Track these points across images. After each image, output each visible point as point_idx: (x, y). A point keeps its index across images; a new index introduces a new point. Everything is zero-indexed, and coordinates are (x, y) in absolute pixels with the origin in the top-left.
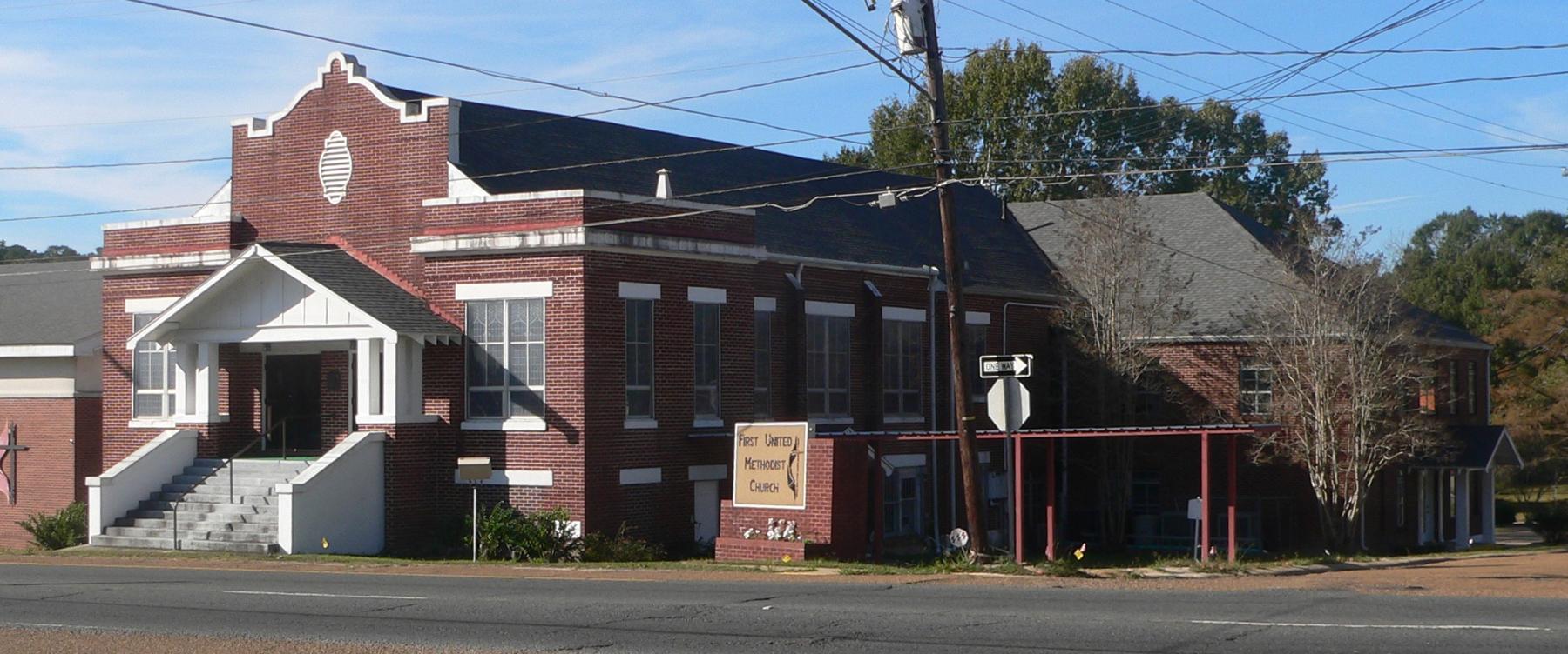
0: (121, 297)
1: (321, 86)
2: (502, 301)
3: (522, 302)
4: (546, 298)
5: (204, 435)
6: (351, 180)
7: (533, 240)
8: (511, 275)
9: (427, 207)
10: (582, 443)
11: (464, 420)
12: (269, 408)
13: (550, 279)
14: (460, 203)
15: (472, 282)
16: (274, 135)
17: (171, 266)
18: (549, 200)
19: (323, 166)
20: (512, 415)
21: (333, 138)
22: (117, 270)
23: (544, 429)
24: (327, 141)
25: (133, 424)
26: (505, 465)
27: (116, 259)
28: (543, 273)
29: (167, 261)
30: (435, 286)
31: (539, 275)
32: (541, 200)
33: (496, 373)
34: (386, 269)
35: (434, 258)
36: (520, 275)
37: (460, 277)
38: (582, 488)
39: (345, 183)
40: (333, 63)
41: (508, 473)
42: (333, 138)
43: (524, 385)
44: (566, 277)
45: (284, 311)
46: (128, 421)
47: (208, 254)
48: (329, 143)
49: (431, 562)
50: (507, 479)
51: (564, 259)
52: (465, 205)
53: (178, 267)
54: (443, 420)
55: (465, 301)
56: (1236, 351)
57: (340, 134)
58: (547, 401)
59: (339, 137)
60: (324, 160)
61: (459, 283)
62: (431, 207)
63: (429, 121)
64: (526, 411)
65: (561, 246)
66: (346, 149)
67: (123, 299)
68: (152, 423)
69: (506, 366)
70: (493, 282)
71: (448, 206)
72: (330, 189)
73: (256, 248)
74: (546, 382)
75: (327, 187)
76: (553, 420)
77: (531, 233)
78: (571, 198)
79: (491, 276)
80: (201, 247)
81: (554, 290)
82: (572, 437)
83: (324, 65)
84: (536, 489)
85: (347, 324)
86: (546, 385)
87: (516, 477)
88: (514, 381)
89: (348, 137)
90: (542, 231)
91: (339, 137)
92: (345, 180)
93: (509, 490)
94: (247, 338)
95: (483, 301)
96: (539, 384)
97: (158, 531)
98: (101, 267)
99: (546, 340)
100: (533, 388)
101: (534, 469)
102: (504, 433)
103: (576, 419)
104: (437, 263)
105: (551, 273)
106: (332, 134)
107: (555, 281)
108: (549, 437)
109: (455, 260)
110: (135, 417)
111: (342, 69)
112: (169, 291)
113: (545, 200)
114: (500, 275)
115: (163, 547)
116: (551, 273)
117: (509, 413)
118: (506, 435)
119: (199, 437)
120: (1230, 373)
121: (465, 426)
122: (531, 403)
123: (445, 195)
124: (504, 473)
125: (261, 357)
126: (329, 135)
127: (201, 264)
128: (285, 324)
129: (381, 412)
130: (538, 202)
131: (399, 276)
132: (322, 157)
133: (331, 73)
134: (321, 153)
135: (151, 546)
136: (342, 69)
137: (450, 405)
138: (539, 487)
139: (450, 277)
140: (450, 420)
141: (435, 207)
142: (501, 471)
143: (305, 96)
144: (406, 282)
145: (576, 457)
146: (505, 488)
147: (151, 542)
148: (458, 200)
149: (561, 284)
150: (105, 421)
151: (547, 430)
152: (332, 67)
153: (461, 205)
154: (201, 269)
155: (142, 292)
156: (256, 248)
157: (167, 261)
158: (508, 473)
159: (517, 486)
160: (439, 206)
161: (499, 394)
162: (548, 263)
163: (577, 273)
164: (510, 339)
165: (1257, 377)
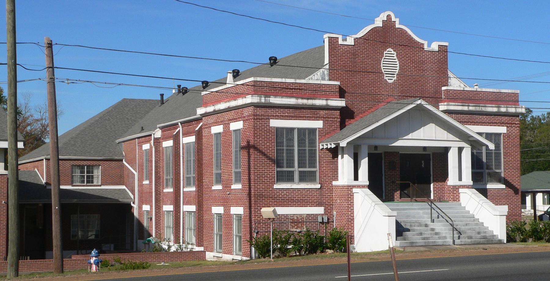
7: (503, 110)
8: (489, 123)
13: (506, 126)
15: (471, 125)
18: (504, 93)
21: (388, 51)
24: (385, 52)
25: (275, 186)
27: (270, 97)
31: (501, 124)
32: (501, 93)
35: (452, 113)
36: (493, 123)
40: (387, 16)
43: (492, 169)
46: (273, 185)
48: (386, 54)
52: (466, 91)
57: (392, 50)
67: (269, 119)
68: (291, 186)
71: (458, 90)
78: (514, 93)
89: (396, 52)
94: (391, 144)
97: (429, 237)
98: (259, 100)
104: (453, 115)
106: (388, 50)
107: (507, 127)
111: (393, 20)
112: (301, 117)
113: (503, 93)
115: (444, 244)
118: (487, 190)
126: (386, 50)
127: (327, 105)
136: (393, 20)
147: (438, 242)
152: (387, 18)
153: (464, 91)
155: (283, 116)
163: (517, 124)
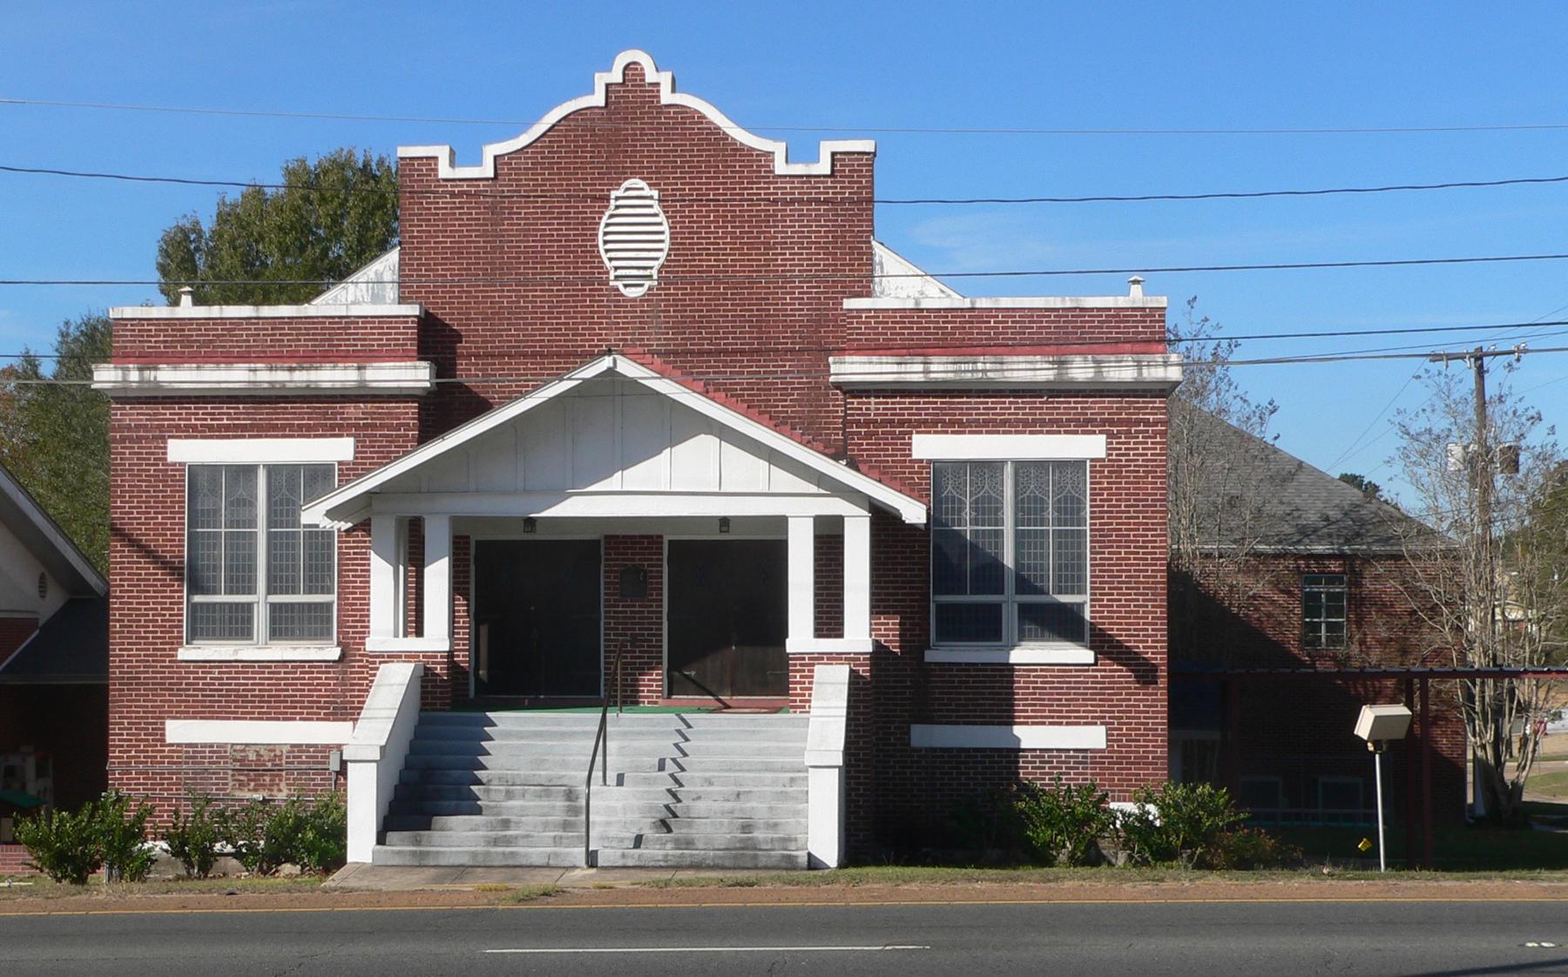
0: (162, 435)
1: (602, 104)
2: (1003, 462)
3: (1041, 465)
4: (340, 463)
5: (438, 671)
6: (667, 260)
7: (1081, 371)
8: (1026, 423)
9: (851, 310)
10: (1163, 682)
11: (929, 648)
12: (484, 629)
13: (1101, 432)
14: (922, 306)
15: (946, 432)
16: (496, 178)
17: (289, 385)
18: (1099, 309)
19: (606, 234)
20: (1021, 640)
21: (627, 189)
22: (1072, 382)
23: (1092, 661)
24: (614, 194)
25: (184, 653)
26: (1014, 717)
27: (156, 369)
28: (1088, 422)
29: (281, 376)
30: (868, 435)
31: (1083, 425)
32: (1082, 309)
33: (990, 575)
34: (745, 405)
35: (869, 391)
36: (1043, 423)
37: (920, 423)
38: (1162, 752)
39: (656, 264)
40: (626, 67)
41: (1018, 730)
42: (627, 189)
43: (1042, 591)
44: (1133, 429)
45: (623, 469)
46: (176, 650)
47: (374, 368)
48: (617, 198)
49: (1545, 874)
50: (1019, 740)
51: (1126, 402)
52: (928, 310)
53: (308, 387)
54: (887, 647)
55: (929, 461)
56: (1298, 567)
57: (643, 184)
58: (1092, 618)
59: (642, 189)
60: (608, 225)
61: (918, 432)
62: (858, 310)
63: (832, 175)
64: (1047, 634)
65: (1136, 382)
66: (657, 209)
67: (164, 439)
68: (236, 652)
69: (1009, 560)
70: (1005, 432)
71: (895, 310)
72: (620, 272)
73: (615, 361)
74: (1092, 588)
75: (616, 268)
76: (1104, 645)
77: (1078, 358)
78: (1143, 309)
79: (986, 423)
80: (364, 357)
81: (1108, 449)
82: (1144, 673)
83: (608, 68)
84: (1072, 753)
85: (766, 491)
86: (1092, 594)
87: (1030, 736)
88: (1024, 585)
89: (660, 190)
90: (1099, 357)
91: (642, 189)
92: (657, 259)
93: (1018, 757)
94: (538, 513)
95: (965, 462)
96: (1079, 593)
97: (516, 837)
99: (1091, 524)
100: (1064, 599)
101: (1033, 723)
102: (1010, 668)
103: (1153, 645)
104: (873, 400)
105: (1104, 422)
106: (626, 184)
107: (1110, 435)
108: (1098, 674)
109: (911, 397)
110: (187, 643)
111: (649, 79)
112: (275, 428)
113: (1092, 309)
114: (1004, 423)
115: (552, 862)
116: (1104, 422)
117: (1016, 638)
118: (1014, 670)
119: (426, 675)
120: (1289, 593)
121: (931, 656)
122: (1065, 624)
123: (869, 295)
124: (1012, 730)
125: (468, 543)
126: (620, 185)
127: (362, 384)
128: (673, 490)
129: (419, 632)
130: (1077, 313)
131: (771, 418)
132: (605, 220)
133: (623, 84)
134: (603, 213)
135: (524, 862)
136: (649, 79)
137: (900, 624)
138: (1076, 750)
139: (902, 423)
140: (900, 647)
141: (869, 310)
142: (1009, 727)
143: (565, 118)
144: (789, 427)
145: (1153, 705)
146: (1014, 753)
147: (526, 855)
148: (917, 303)
149: (1123, 440)
150: (115, 650)
151: (1096, 664)
152: (624, 75)
153: (922, 310)
154: (362, 392)
155: (211, 428)
156: (615, 361)
157: (281, 376)
158: (1018, 730)
159: (1034, 750)
160: (876, 310)
161: (996, 608)
162: (1095, 406)
163: (1155, 423)
164: (270, 524)
165: (1324, 600)
